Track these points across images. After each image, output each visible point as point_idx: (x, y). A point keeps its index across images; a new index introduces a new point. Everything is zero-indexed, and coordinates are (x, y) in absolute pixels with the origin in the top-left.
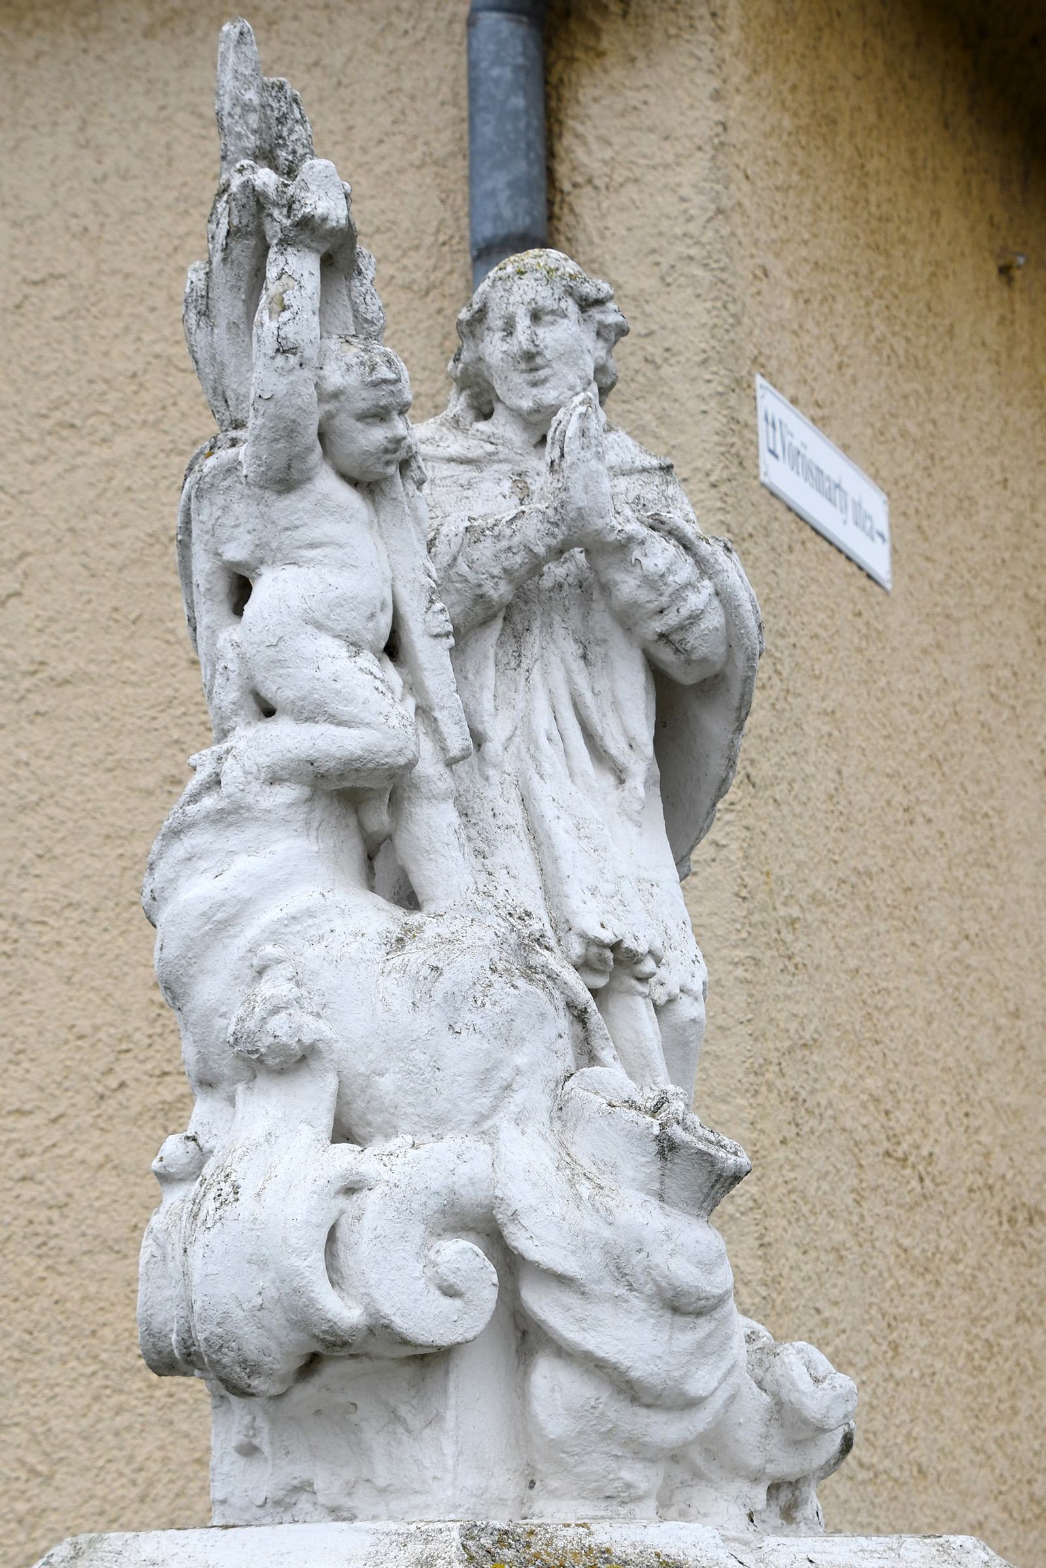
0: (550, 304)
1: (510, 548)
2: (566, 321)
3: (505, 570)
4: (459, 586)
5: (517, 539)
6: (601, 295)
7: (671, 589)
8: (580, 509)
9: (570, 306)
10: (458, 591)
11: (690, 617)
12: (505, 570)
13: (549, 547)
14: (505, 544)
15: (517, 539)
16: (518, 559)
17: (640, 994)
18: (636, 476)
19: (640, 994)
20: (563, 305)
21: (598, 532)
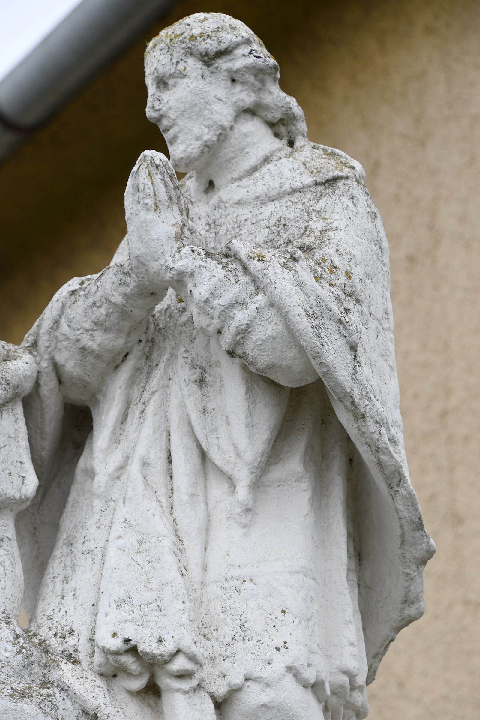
0: (169, 69)
1: (94, 303)
2: (186, 80)
3: (95, 323)
4: (65, 343)
5: (99, 293)
6: (223, 46)
7: (216, 313)
8: (137, 257)
9: (193, 65)
10: (66, 348)
11: (238, 334)
12: (95, 323)
13: (125, 295)
14: (91, 300)
15: (99, 293)
16: (103, 311)
17: (178, 690)
18: (287, 198)
19: (178, 690)
20: (181, 67)
21: (157, 273)
